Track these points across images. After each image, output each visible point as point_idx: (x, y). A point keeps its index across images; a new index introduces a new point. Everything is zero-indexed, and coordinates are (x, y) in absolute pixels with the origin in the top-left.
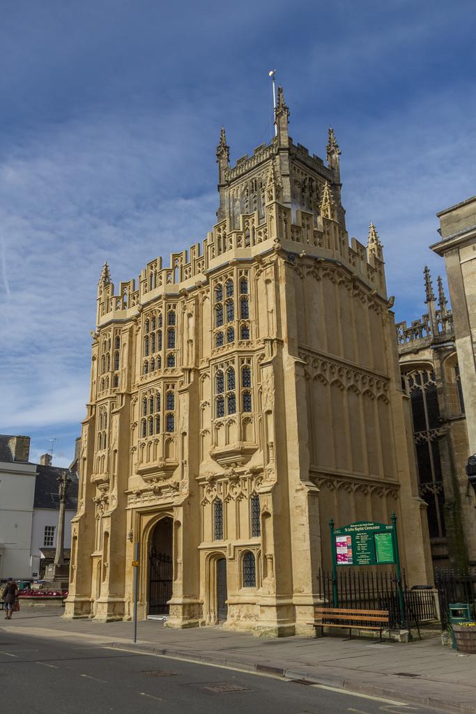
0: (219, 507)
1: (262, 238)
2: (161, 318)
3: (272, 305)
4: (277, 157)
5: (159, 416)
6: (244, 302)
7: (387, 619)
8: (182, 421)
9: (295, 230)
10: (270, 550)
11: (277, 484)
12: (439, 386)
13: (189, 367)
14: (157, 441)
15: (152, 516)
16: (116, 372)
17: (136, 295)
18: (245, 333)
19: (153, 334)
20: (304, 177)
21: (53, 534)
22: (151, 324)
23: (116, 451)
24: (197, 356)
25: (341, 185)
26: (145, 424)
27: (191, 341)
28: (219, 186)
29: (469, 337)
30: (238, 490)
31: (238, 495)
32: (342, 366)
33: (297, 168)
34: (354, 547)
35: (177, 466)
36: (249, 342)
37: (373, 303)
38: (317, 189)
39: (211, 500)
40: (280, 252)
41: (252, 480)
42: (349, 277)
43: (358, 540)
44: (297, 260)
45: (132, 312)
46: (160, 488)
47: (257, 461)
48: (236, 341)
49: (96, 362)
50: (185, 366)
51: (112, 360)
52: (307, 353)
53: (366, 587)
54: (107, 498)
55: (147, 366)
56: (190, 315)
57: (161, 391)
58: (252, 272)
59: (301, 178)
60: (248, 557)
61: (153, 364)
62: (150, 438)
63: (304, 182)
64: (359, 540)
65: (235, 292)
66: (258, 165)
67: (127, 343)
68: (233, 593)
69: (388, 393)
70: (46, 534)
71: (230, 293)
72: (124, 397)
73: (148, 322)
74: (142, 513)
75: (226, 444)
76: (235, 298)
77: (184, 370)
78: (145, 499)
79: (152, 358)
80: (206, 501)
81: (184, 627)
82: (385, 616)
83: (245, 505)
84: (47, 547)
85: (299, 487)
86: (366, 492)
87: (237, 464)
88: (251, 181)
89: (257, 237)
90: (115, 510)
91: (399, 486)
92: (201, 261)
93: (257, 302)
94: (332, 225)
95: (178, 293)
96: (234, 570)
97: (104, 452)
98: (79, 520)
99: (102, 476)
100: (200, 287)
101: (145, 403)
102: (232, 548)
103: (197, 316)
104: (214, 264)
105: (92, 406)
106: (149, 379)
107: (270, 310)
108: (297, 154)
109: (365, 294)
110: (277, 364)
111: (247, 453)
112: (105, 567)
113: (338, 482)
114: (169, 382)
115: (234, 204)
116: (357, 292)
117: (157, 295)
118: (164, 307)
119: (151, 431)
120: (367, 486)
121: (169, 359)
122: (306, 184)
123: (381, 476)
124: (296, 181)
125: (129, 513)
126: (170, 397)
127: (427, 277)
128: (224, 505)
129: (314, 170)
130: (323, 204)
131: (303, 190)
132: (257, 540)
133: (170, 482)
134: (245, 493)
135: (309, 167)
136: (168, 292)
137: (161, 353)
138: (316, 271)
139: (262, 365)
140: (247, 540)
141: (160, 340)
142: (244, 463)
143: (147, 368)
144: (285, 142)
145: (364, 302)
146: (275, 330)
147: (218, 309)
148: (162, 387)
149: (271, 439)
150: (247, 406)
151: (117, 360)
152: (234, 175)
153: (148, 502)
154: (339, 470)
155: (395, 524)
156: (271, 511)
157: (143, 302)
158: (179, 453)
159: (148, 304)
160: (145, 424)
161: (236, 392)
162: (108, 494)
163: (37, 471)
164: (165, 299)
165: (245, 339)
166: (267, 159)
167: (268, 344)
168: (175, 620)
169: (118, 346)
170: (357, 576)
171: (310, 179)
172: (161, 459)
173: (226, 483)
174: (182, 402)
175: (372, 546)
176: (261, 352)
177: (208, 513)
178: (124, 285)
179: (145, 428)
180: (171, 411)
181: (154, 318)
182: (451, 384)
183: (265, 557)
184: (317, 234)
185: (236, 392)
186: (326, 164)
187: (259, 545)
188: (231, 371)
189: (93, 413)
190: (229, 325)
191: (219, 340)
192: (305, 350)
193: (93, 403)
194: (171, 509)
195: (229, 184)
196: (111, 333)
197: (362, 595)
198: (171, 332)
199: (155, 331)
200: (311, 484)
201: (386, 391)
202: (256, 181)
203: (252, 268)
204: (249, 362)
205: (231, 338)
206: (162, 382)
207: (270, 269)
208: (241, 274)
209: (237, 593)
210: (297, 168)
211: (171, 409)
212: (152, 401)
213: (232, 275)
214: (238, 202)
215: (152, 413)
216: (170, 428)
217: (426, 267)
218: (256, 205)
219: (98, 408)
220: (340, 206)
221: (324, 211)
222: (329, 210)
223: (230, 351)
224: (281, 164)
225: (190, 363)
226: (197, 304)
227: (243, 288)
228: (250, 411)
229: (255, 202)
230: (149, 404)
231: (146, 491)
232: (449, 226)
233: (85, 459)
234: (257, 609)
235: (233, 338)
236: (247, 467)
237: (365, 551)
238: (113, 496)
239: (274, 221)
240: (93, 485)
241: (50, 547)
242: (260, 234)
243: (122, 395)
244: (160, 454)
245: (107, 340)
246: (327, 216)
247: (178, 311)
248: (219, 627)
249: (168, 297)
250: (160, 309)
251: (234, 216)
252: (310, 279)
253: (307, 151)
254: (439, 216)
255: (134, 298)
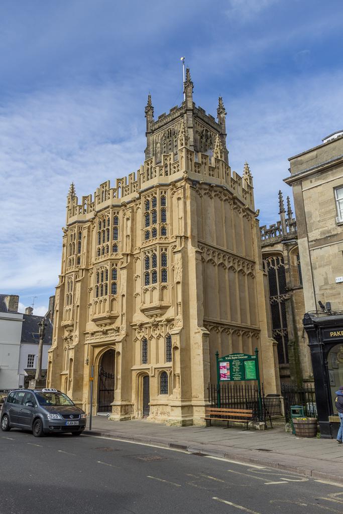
0: (145, 342)
1: (176, 170)
2: (109, 221)
3: (182, 214)
4: (185, 115)
5: (107, 284)
6: (163, 211)
7: (251, 415)
8: (122, 288)
9: (197, 166)
10: (178, 371)
11: (183, 328)
12: (286, 267)
13: (127, 253)
14: (106, 300)
15: (102, 348)
16: (79, 255)
17: (92, 205)
18: (164, 231)
19: (104, 231)
20: (202, 129)
21: (33, 360)
22: (102, 224)
23: (78, 306)
24: (132, 246)
25: (226, 135)
26: (98, 289)
27: (129, 236)
28: (146, 133)
29: (307, 238)
30: (157, 332)
31: (157, 335)
32: (225, 253)
34: (231, 369)
35: (118, 316)
36: (166, 237)
37: (245, 213)
38: (211, 137)
39: (140, 338)
40: (188, 180)
41: (167, 326)
42: (231, 197)
43: (234, 365)
44: (198, 185)
45: (90, 216)
46: (107, 330)
47: (170, 314)
48: (158, 236)
49: (65, 248)
50: (124, 252)
51: (76, 247)
52: (203, 245)
53: (238, 395)
54: (72, 336)
55: (99, 251)
56: (128, 219)
57: (108, 268)
58: (169, 193)
59: (200, 129)
60: (163, 375)
61: (103, 250)
62: (101, 298)
63: (202, 132)
64: (235, 365)
65: (158, 205)
66: (172, 120)
67: (86, 236)
68: (154, 398)
69: (254, 271)
70: (29, 360)
71: (154, 205)
72: (84, 271)
73: (100, 223)
74: (95, 346)
75: (150, 303)
76: (158, 208)
77: (123, 255)
78: (97, 337)
79: (103, 246)
80: (137, 339)
81: (121, 420)
82: (250, 413)
83: (162, 342)
84: (29, 368)
85: (197, 331)
86: (239, 334)
87: (157, 316)
88: (168, 130)
89: (173, 169)
90: (77, 344)
91: (260, 330)
92: (135, 184)
93: (172, 211)
94: (221, 163)
95: (120, 204)
96: (154, 383)
97: (71, 307)
98: (53, 351)
99: (69, 323)
100: (134, 201)
101: (98, 275)
102: (153, 369)
103: (133, 220)
104: (144, 186)
105: (62, 277)
106: (101, 260)
107: (180, 217)
108: (198, 114)
109: (240, 208)
110: (184, 252)
111: (164, 308)
112: (70, 381)
113: (221, 328)
114: (114, 262)
115: (156, 145)
116: (236, 206)
117: (106, 206)
118: (111, 213)
119: (102, 294)
120: (239, 330)
121: (114, 247)
123: (248, 324)
124: (197, 132)
125: (86, 346)
126: (114, 271)
127: (280, 198)
128: (148, 341)
129: (209, 125)
130: (215, 149)
131: (201, 138)
132: (170, 364)
133: (113, 326)
134: (163, 335)
135: (205, 122)
136: (114, 204)
137: (109, 243)
138: (210, 192)
139: (174, 252)
140: (163, 364)
141: (108, 235)
142: (162, 315)
143: (100, 252)
144: (190, 106)
145: (240, 213)
146: (183, 230)
147: (147, 216)
148: (109, 265)
149: (180, 300)
150: (164, 279)
151: (80, 247)
152: (156, 126)
153: (99, 339)
154: (222, 320)
155: (257, 355)
156: (179, 346)
157: (97, 210)
158: (120, 307)
159: (101, 211)
160: (98, 289)
161: (157, 269)
162: (73, 334)
163: (23, 319)
164: (112, 208)
165: (164, 235)
166: (178, 117)
167: (179, 239)
168: (116, 416)
169: (80, 238)
170: (232, 388)
171: (206, 130)
172: (108, 312)
173: (150, 327)
174: (122, 275)
175: (243, 369)
176: (174, 244)
177: (138, 346)
178: (85, 198)
179: (97, 292)
180: (114, 281)
181: (104, 221)
182: (294, 266)
183: (174, 375)
184: (211, 169)
185: (157, 269)
186: (217, 121)
187: (171, 367)
188: (154, 256)
189: (63, 281)
190: (153, 226)
191: (147, 236)
192: (202, 243)
193: (63, 275)
194: (114, 344)
195: (153, 132)
196: (76, 230)
197: (236, 400)
198: (115, 229)
199: (105, 229)
200: (204, 329)
201: (252, 270)
202: (171, 131)
203: (169, 190)
204: (166, 250)
205: (154, 234)
206: (109, 262)
207: (181, 191)
208: (162, 193)
209: (156, 397)
211: (115, 279)
212: (102, 274)
213: (156, 194)
214: (159, 145)
215: (102, 281)
216: (114, 292)
217: (280, 191)
218: (170, 147)
219: (66, 278)
220: (225, 149)
221: (216, 153)
222: (219, 153)
223: (154, 243)
224: (187, 120)
225: (128, 250)
226: (133, 212)
227: (163, 203)
228: (166, 282)
229: (170, 144)
230: (101, 276)
231: (98, 332)
232: (296, 167)
233: (57, 311)
234: (168, 409)
235: (156, 234)
236: (164, 318)
237: (238, 372)
238: (76, 336)
239: (184, 159)
240: (62, 328)
241: (31, 368)
242: (175, 168)
243: (83, 270)
244: (107, 309)
245: (73, 234)
246: (218, 157)
247: (120, 216)
248: (145, 420)
249: (114, 206)
250: (108, 215)
251: (156, 154)
252: (206, 197)
253: (204, 111)
254: (289, 160)
255: (91, 207)
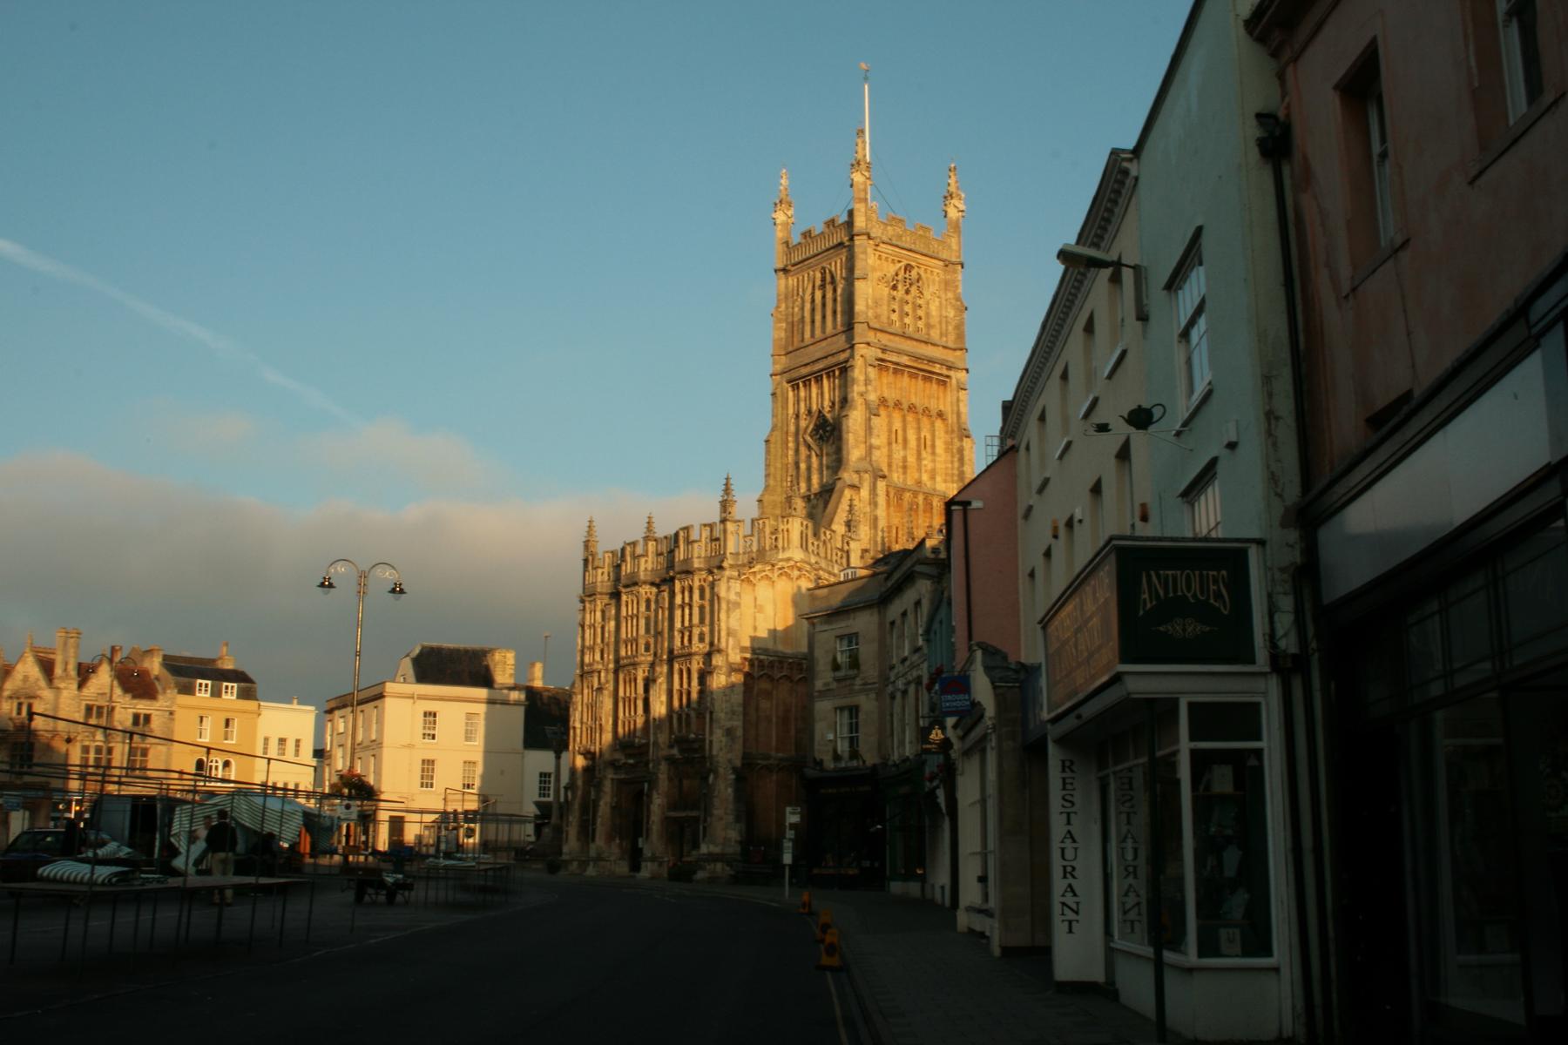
33: (884, 256)
63: (897, 275)
84: (543, 799)
122: (900, 277)
210: (884, 256)
